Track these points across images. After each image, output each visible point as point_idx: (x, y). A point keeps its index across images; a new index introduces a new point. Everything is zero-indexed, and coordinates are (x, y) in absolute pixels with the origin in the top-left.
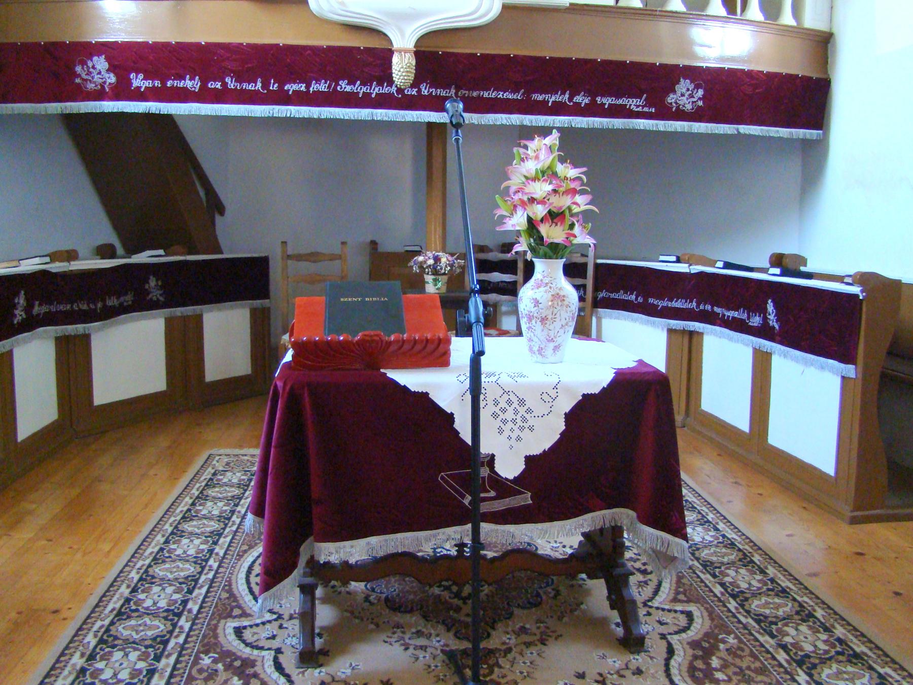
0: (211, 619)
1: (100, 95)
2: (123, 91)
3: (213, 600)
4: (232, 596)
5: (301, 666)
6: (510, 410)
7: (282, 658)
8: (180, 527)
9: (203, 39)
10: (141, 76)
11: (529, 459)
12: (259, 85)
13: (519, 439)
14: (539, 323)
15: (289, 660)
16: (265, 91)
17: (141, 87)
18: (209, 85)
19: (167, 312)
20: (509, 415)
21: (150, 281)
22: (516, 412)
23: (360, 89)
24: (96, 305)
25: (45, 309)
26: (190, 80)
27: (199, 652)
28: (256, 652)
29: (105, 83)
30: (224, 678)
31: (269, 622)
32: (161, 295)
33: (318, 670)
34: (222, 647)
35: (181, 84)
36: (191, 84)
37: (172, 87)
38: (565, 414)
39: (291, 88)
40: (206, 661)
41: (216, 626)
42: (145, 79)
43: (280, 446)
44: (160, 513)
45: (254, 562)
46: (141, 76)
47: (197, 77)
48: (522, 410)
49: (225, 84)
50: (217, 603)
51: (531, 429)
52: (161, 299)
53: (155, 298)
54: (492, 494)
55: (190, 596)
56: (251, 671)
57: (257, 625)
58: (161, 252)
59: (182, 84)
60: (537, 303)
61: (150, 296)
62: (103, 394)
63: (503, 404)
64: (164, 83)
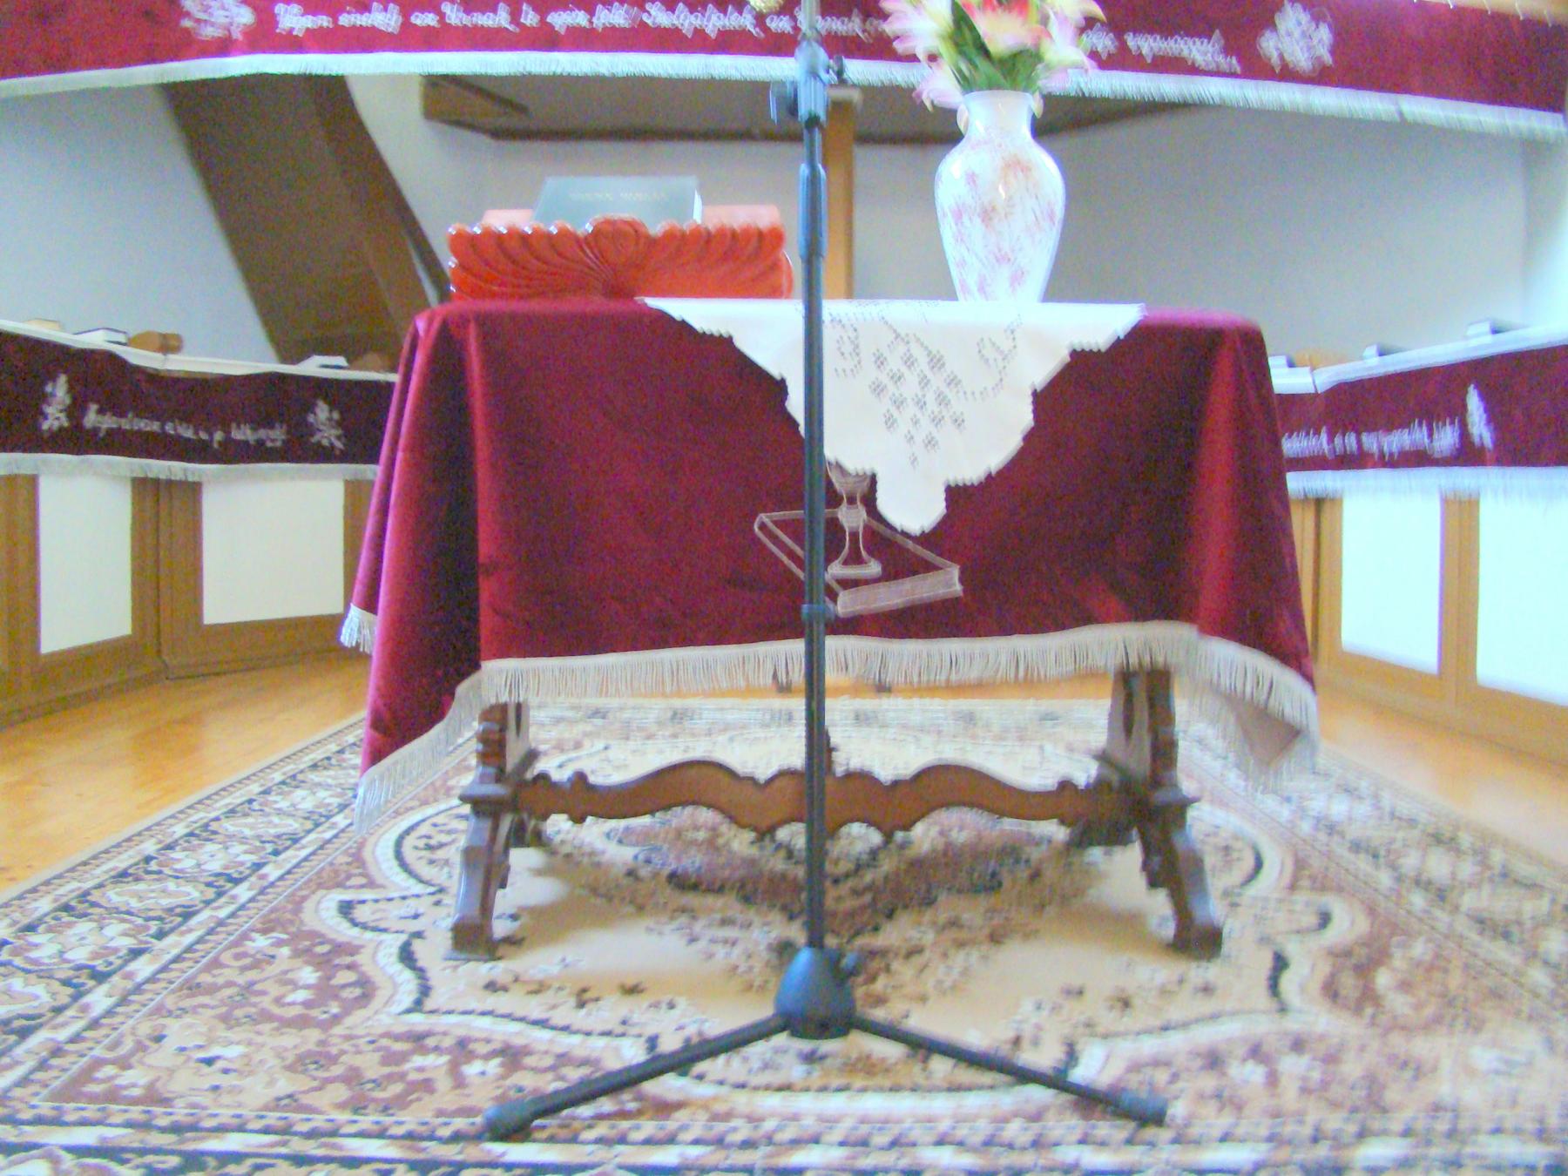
0: (300, 889)
1: (223, 47)
2: (265, 37)
3: (319, 862)
4: (357, 858)
5: (455, 955)
6: (911, 379)
7: (417, 945)
8: (300, 777)
11: (956, 495)
13: (930, 443)
14: (977, 221)
15: (435, 949)
20: (910, 387)
21: (318, 410)
22: (924, 382)
23: (684, 20)
24: (211, 435)
25: (108, 422)
27: (253, 930)
28: (369, 935)
29: (231, 24)
30: (284, 967)
31: (418, 896)
32: (338, 438)
33: (489, 965)
34: (302, 922)
35: (363, 20)
36: (384, 19)
38: (1035, 394)
39: (561, 20)
40: (261, 942)
41: (304, 898)
43: (411, 448)
45: (423, 821)
48: (937, 381)
49: (442, 16)
50: (323, 869)
51: (958, 422)
52: (339, 445)
53: (325, 442)
54: (873, 568)
55: (273, 858)
56: (348, 960)
57: (390, 900)
58: (341, 360)
60: (972, 178)
62: (219, 607)
63: (894, 363)
64: (336, 21)
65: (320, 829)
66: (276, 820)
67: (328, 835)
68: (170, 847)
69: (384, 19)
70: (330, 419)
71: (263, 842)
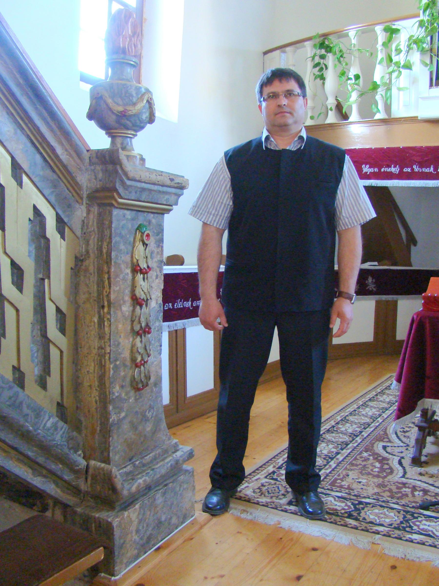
0: (372, 440)
3: (375, 433)
4: (386, 433)
5: (412, 464)
7: (403, 460)
8: (367, 403)
9: (401, 145)
10: (368, 166)
12: (432, 169)
15: (407, 462)
16: (435, 173)
17: (367, 172)
18: (404, 170)
19: (378, 297)
21: (369, 279)
26: (394, 167)
27: (363, 451)
28: (390, 456)
30: (372, 462)
31: (402, 446)
32: (374, 287)
33: (420, 468)
34: (374, 450)
35: (389, 170)
36: (394, 170)
37: (384, 171)
40: (365, 454)
41: (374, 443)
42: (370, 167)
44: (358, 396)
46: (368, 166)
47: (398, 166)
49: (412, 169)
50: (377, 435)
52: (374, 289)
53: (371, 289)
55: (364, 430)
56: (386, 462)
57: (395, 447)
58: (376, 263)
59: (389, 170)
61: (368, 288)
64: (380, 170)
65: (375, 422)
66: (363, 418)
67: (377, 424)
68: (337, 423)
69: (394, 170)
70: (372, 282)
71: (361, 425)
